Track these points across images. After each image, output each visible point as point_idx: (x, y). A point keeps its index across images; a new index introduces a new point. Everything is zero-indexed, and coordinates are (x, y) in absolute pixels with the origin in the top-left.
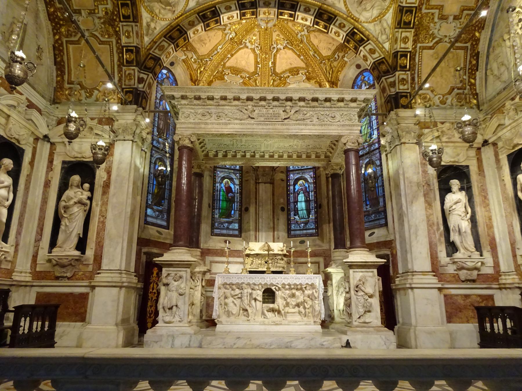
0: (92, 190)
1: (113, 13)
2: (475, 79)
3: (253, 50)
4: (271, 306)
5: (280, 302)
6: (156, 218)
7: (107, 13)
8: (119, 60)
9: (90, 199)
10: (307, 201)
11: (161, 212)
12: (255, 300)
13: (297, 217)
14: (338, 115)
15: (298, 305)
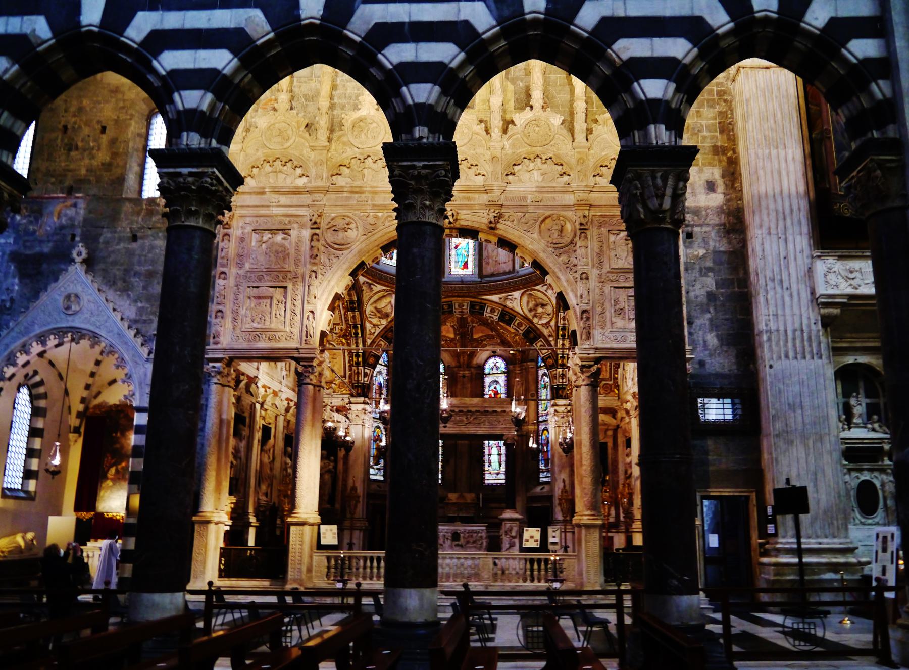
0: (336, 462)
1: (346, 330)
2: (617, 374)
3: (453, 326)
4: (457, 543)
5: (462, 541)
6: (376, 475)
7: (342, 330)
8: (349, 362)
9: (335, 467)
10: (500, 455)
11: (378, 469)
12: (448, 539)
13: (490, 468)
14: (502, 419)
15: (474, 542)
